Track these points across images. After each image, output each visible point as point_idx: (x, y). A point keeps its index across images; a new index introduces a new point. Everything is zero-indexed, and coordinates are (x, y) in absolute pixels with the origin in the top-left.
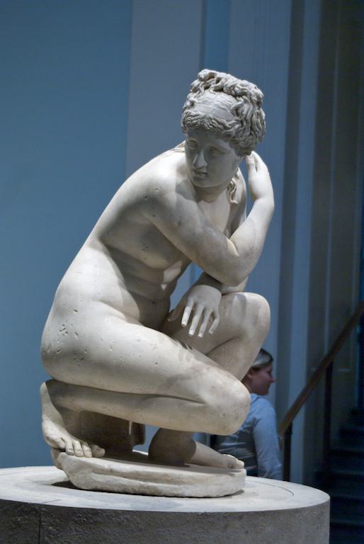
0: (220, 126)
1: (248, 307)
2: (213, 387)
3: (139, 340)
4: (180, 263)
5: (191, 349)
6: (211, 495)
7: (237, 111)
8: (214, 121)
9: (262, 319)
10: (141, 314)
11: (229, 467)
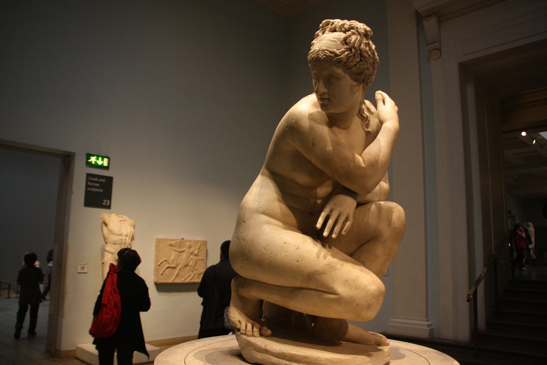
0: (331, 55)
2: (346, 280)
3: (285, 243)
4: (329, 183)
5: (330, 247)
7: (345, 41)
8: (326, 51)
9: (395, 222)
10: (298, 223)
11: (376, 344)
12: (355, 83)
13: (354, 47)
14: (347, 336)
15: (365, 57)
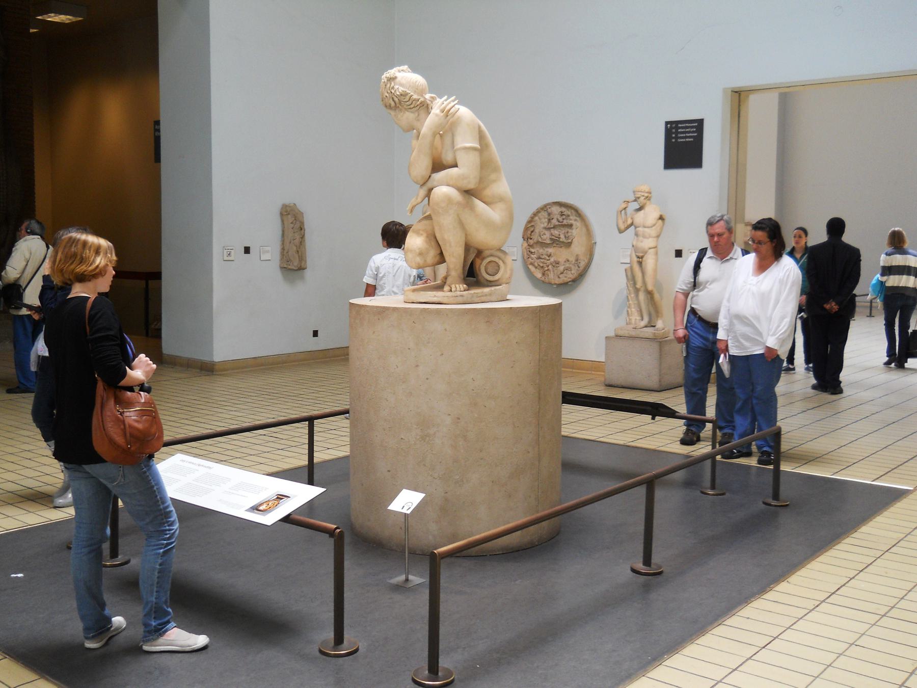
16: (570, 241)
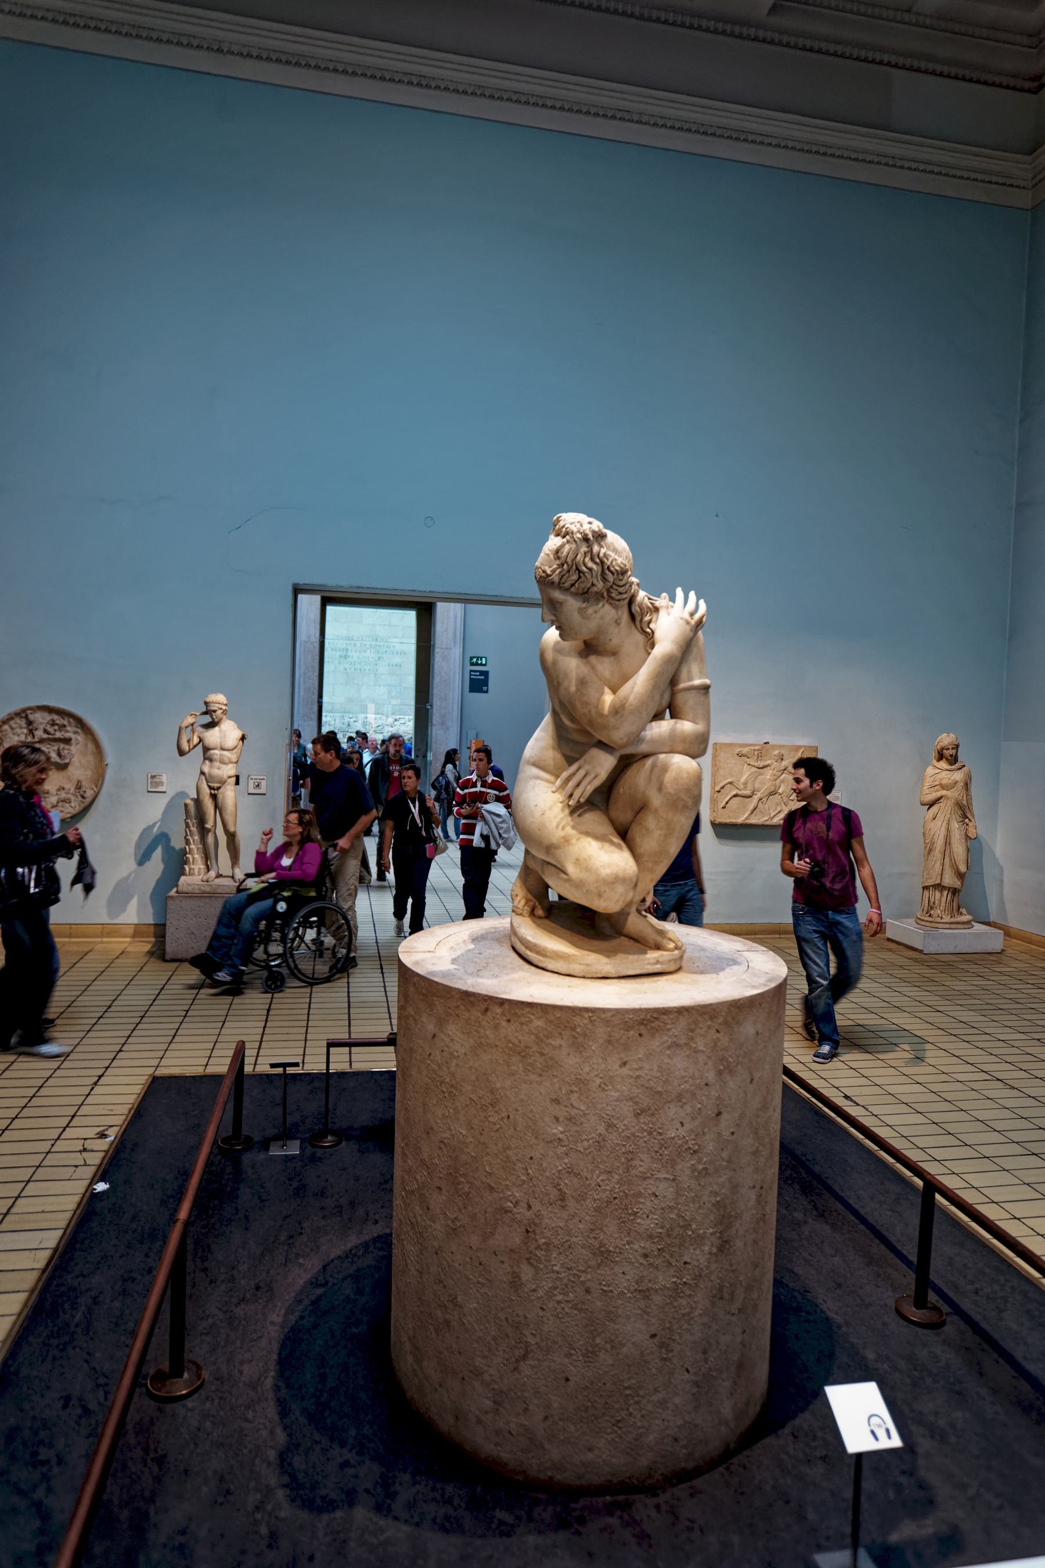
1: (656, 770)
2: (578, 860)
6: (573, 973)
12: (584, 605)
13: (566, 562)
14: (625, 931)
15: (583, 573)
16: (67, 761)
